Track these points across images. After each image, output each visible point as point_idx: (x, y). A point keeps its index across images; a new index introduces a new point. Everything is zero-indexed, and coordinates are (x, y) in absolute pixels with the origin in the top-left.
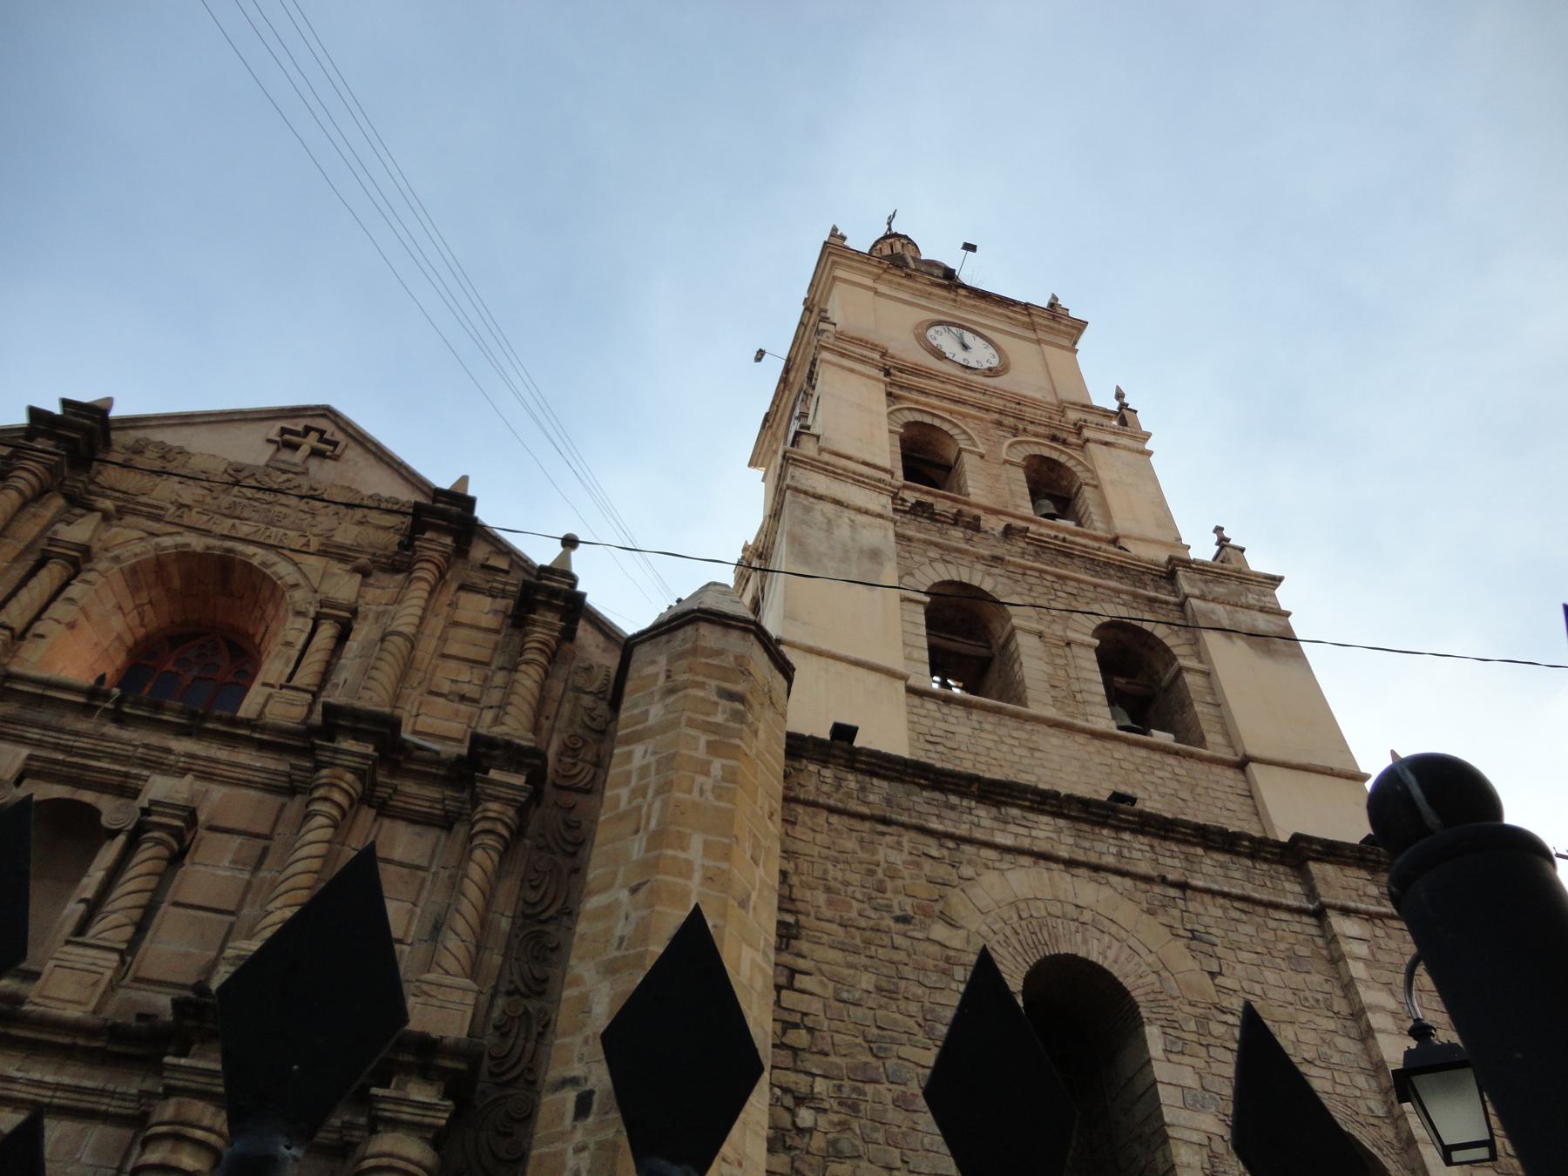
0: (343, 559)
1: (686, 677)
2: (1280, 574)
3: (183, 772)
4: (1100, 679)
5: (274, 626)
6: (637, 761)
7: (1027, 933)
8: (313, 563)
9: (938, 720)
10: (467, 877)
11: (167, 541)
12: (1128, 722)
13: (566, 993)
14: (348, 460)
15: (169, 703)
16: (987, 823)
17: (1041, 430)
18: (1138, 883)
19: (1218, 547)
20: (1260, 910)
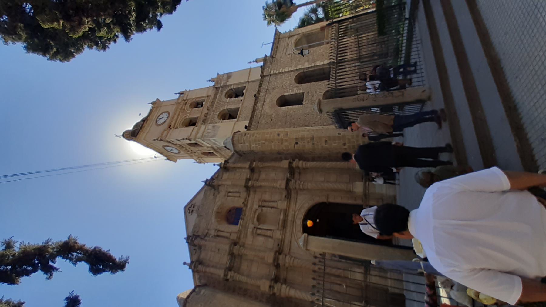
0: (217, 196)
2: (217, 74)
3: (253, 205)
8: (217, 200)
12: (241, 96)
13: (284, 149)
16: (259, 111)
17: (184, 106)
20: (270, 82)
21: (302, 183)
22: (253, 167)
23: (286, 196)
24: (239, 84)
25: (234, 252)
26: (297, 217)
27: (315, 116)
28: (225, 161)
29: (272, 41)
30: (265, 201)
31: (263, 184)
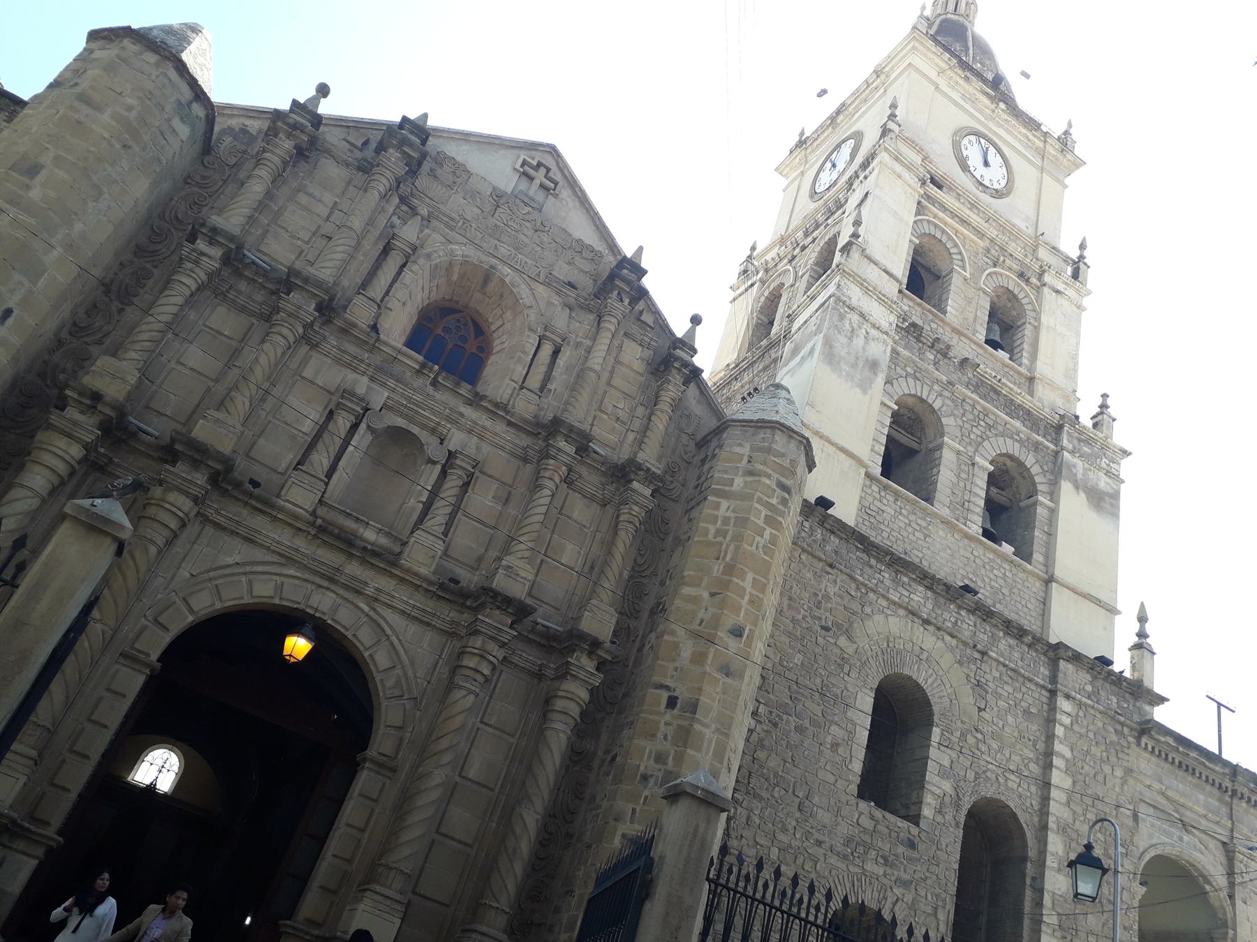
0: (559, 293)
1: (761, 467)
2: (1129, 450)
3: (470, 432)
4: (984, 497)
5: (508, 325)
6: (722, 511)
7: (889, 656)
8: (541, 290)
9: (875, 498)
10: (615, 545)
11: (459, 250)
12: (988, 526)
13: (666, 637)
14: (563, 199)
15: (464, 384)
16: (887, 582)
18: (960, 644)
19: (1099, 410)
20: (1021, 679)
21: (486, 671)
22: (630, 481)
23: (455, 581)
24: (1051, 535)
25: (295, 296)
26: (345, 599)
27: (781, 837)
28: (697, 372)
29: (1225, 756)
30: (466, 485)
31: (544, 497)
